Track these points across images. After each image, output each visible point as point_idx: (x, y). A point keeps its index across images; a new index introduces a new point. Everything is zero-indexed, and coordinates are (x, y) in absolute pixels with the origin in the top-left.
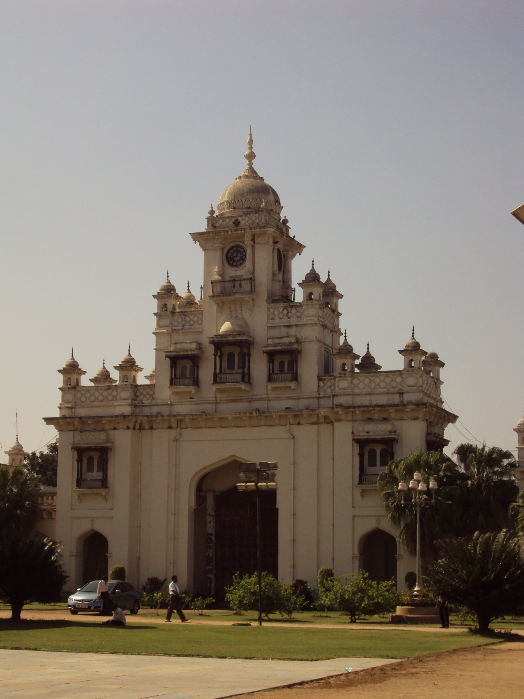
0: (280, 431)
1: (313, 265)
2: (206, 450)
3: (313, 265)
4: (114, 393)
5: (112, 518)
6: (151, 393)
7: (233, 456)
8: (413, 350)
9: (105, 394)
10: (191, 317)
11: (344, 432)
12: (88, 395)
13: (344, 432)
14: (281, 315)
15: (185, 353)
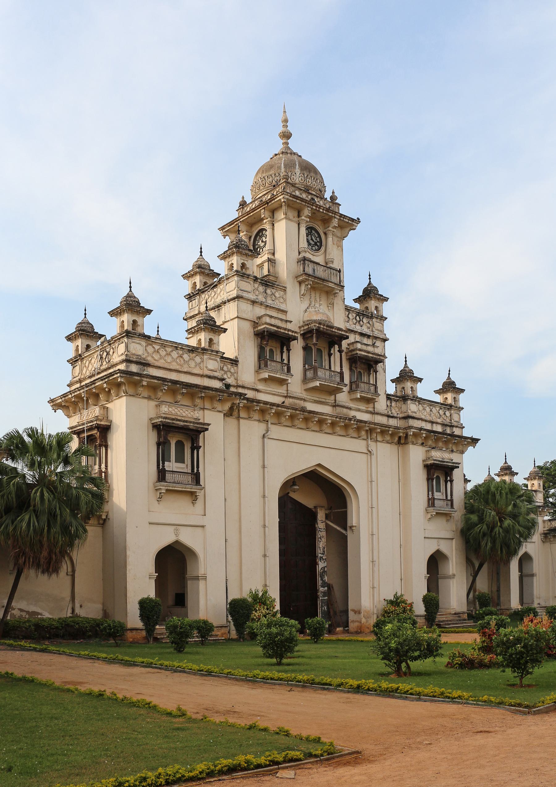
0: (360, 445)
1: (370, 279)
2: (296, 452)
3: (370, 279)
4: (198, 359)
5: (203, 527)
6: (232, 370)
7: (319, 465)
8: (449, 386)
9: (186, 356)
10: (274, 291)
11: (417, 454)
12: (163, 353)
13: (417, 454)
14: (355, 321)
15: (287, 332)
